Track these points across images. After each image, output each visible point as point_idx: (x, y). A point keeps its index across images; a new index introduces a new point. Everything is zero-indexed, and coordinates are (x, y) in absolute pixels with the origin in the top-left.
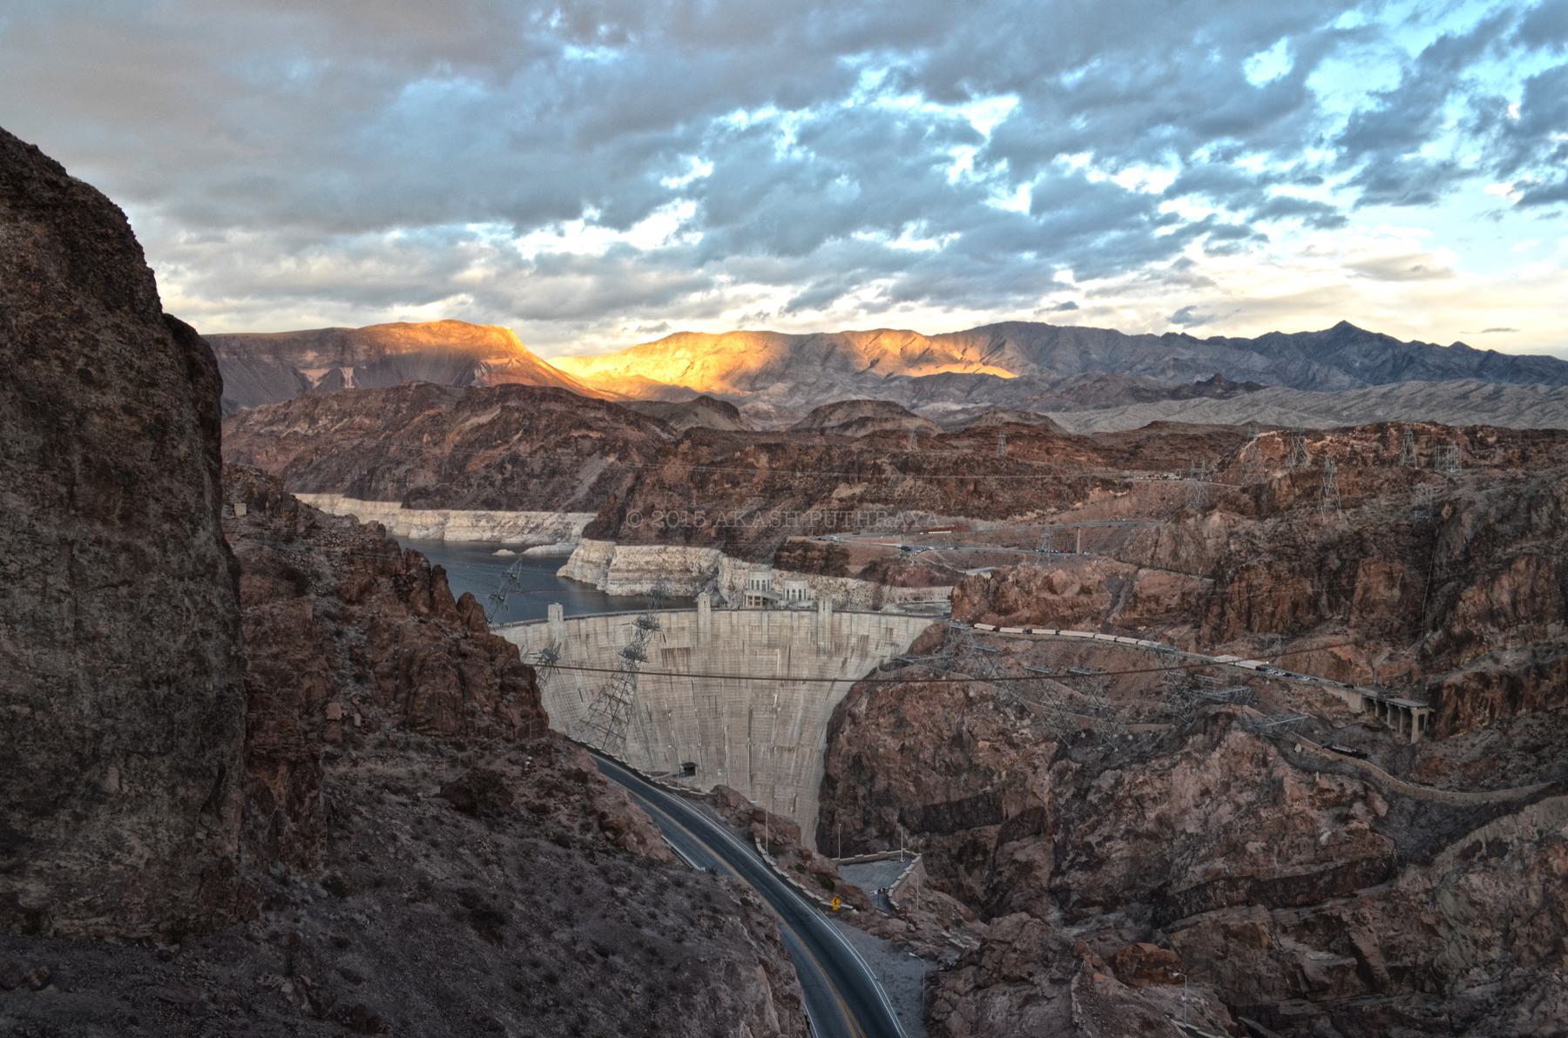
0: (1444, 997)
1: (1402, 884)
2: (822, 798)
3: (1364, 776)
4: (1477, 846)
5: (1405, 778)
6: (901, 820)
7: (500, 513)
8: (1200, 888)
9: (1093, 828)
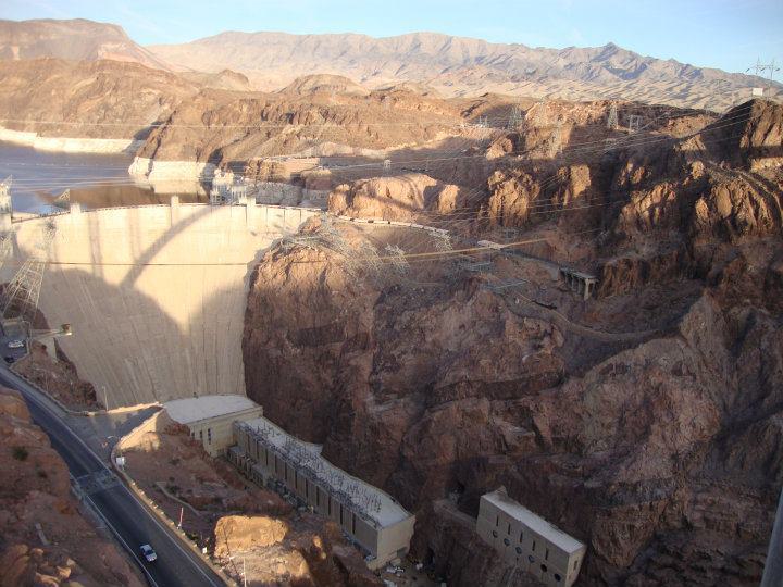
0: (581, 456)
1: (566, 388)
2: (246, 321)
3: (552, 320)
4: (611, 367)
5: (577, 322)
6: (288, 337)
7: (97, 140)
8: (452, 386)
9: (396, 346)
